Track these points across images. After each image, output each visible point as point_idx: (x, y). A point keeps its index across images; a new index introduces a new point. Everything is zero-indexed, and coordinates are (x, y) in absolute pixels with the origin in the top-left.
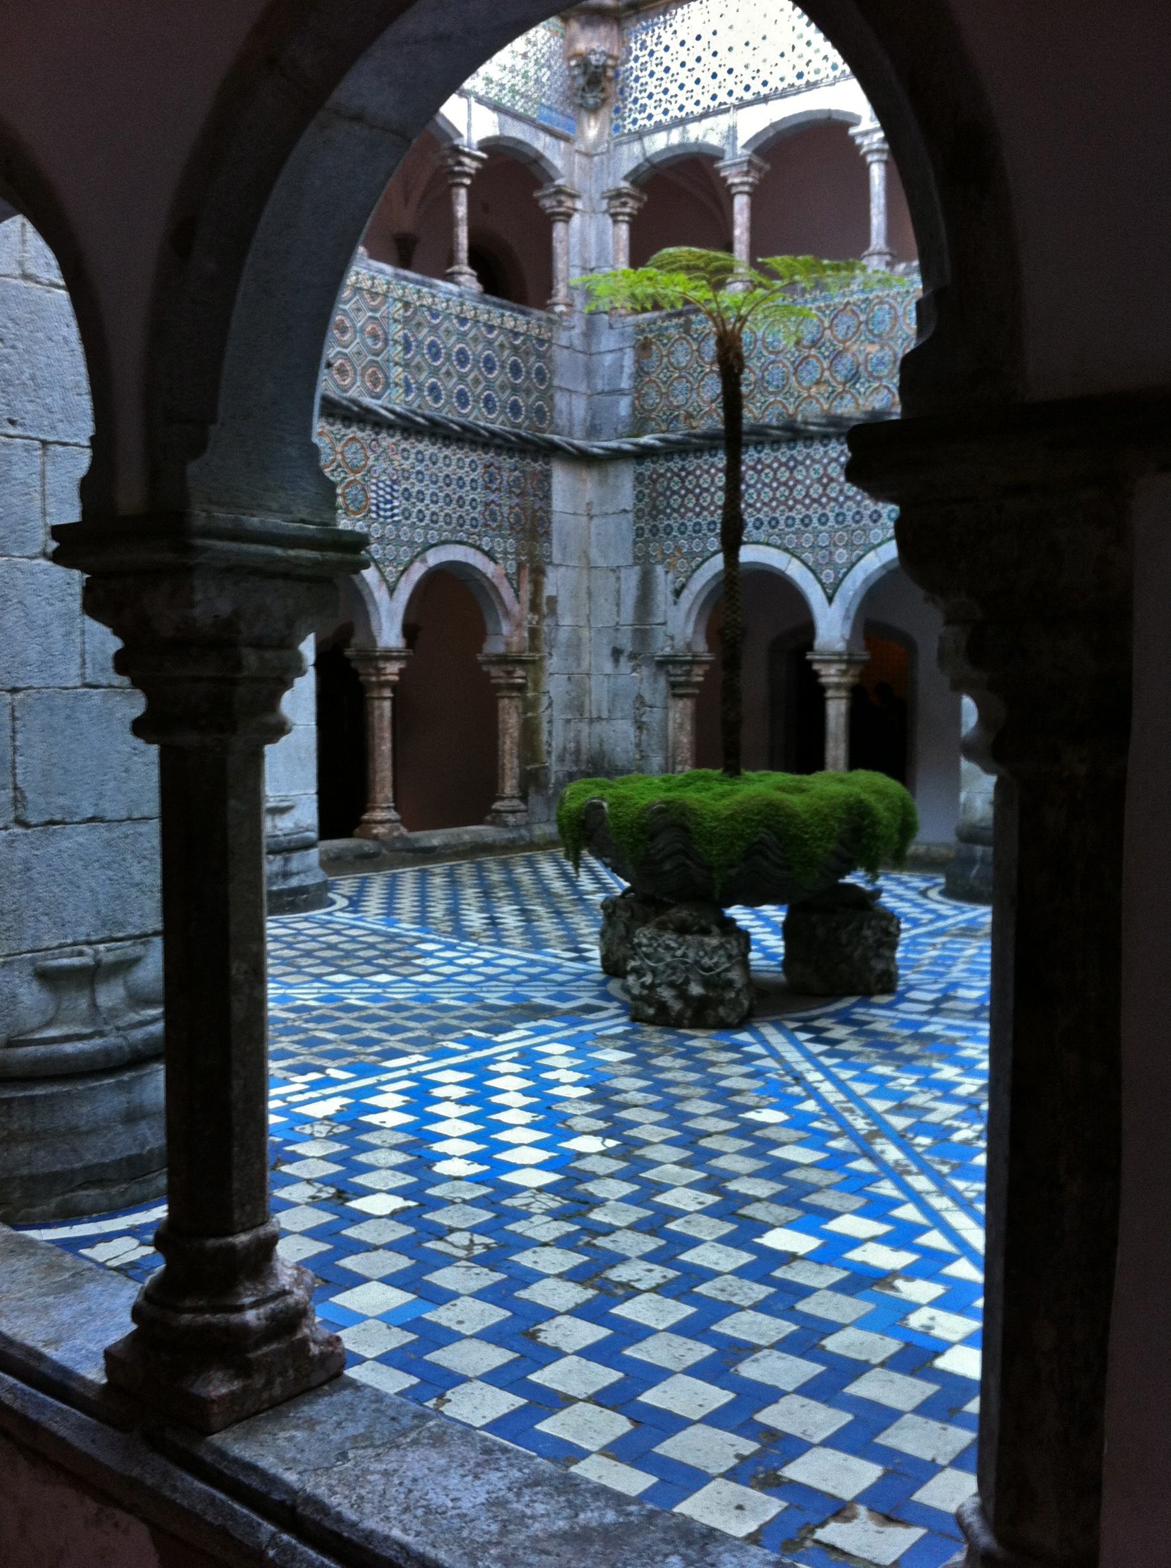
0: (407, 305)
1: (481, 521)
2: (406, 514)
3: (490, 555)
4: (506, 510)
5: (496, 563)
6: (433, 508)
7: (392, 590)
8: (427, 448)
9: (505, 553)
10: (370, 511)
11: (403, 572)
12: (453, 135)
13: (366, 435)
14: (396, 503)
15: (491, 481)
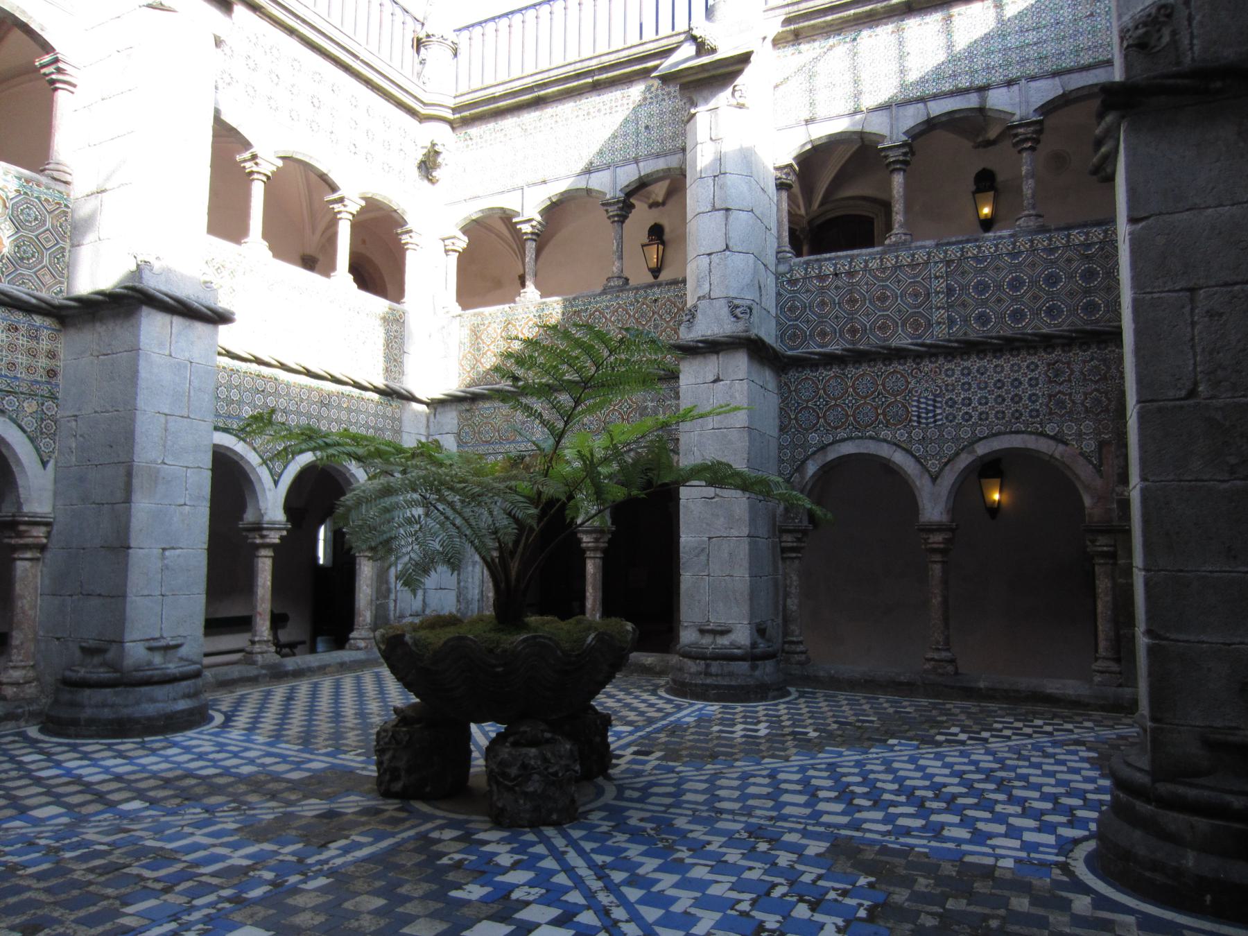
0: (948, 263)
1: (1044, 410)
2: (951, 418)
3: (1058, 439)
4: (1079, 398)
5: (1066, 443)
6: (981, 408)
7: (934, 479)
8: (974, 363)
9: (1080, 435)
10: (911, 421)
11: (946, 464)
12: (1008, 117)
13: (910, 363)
14: (938, 411)
15: (1056, 376)
